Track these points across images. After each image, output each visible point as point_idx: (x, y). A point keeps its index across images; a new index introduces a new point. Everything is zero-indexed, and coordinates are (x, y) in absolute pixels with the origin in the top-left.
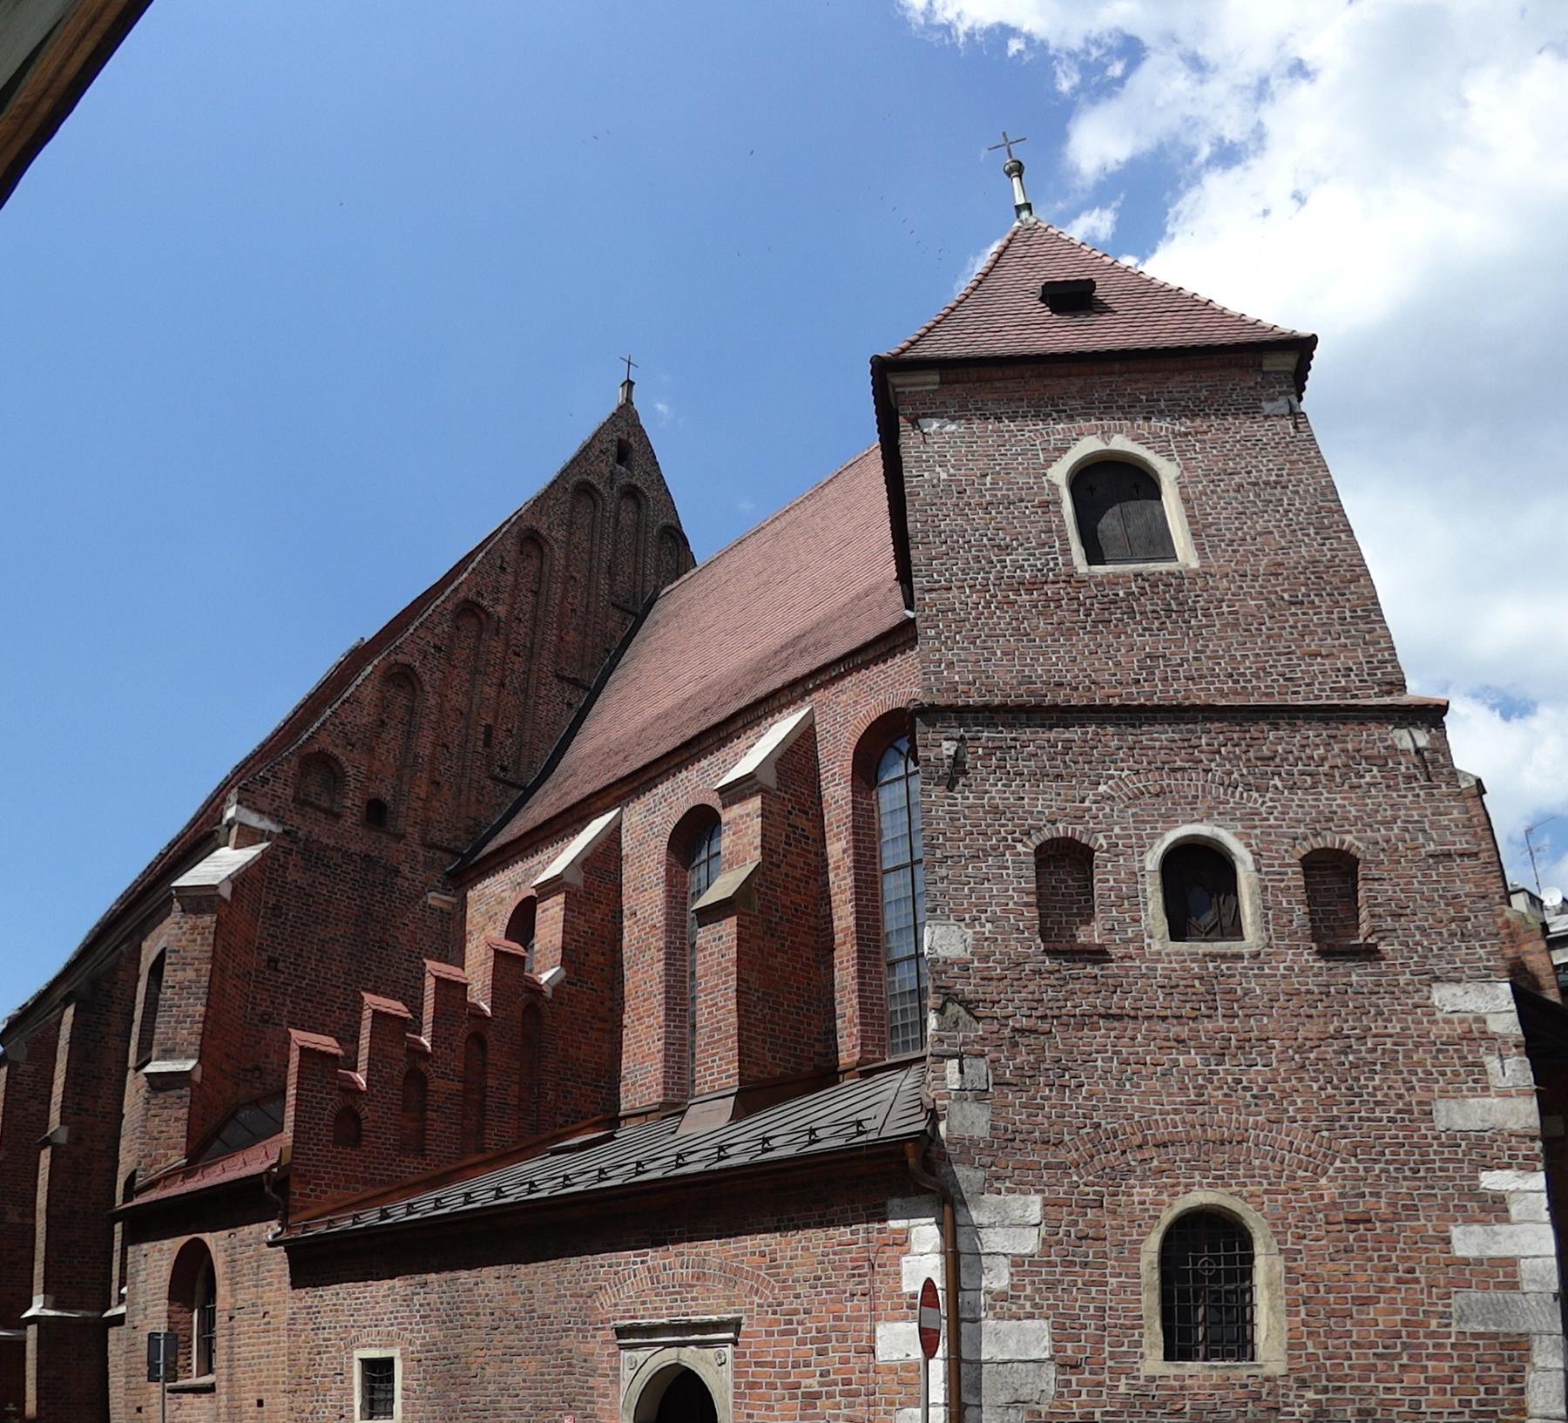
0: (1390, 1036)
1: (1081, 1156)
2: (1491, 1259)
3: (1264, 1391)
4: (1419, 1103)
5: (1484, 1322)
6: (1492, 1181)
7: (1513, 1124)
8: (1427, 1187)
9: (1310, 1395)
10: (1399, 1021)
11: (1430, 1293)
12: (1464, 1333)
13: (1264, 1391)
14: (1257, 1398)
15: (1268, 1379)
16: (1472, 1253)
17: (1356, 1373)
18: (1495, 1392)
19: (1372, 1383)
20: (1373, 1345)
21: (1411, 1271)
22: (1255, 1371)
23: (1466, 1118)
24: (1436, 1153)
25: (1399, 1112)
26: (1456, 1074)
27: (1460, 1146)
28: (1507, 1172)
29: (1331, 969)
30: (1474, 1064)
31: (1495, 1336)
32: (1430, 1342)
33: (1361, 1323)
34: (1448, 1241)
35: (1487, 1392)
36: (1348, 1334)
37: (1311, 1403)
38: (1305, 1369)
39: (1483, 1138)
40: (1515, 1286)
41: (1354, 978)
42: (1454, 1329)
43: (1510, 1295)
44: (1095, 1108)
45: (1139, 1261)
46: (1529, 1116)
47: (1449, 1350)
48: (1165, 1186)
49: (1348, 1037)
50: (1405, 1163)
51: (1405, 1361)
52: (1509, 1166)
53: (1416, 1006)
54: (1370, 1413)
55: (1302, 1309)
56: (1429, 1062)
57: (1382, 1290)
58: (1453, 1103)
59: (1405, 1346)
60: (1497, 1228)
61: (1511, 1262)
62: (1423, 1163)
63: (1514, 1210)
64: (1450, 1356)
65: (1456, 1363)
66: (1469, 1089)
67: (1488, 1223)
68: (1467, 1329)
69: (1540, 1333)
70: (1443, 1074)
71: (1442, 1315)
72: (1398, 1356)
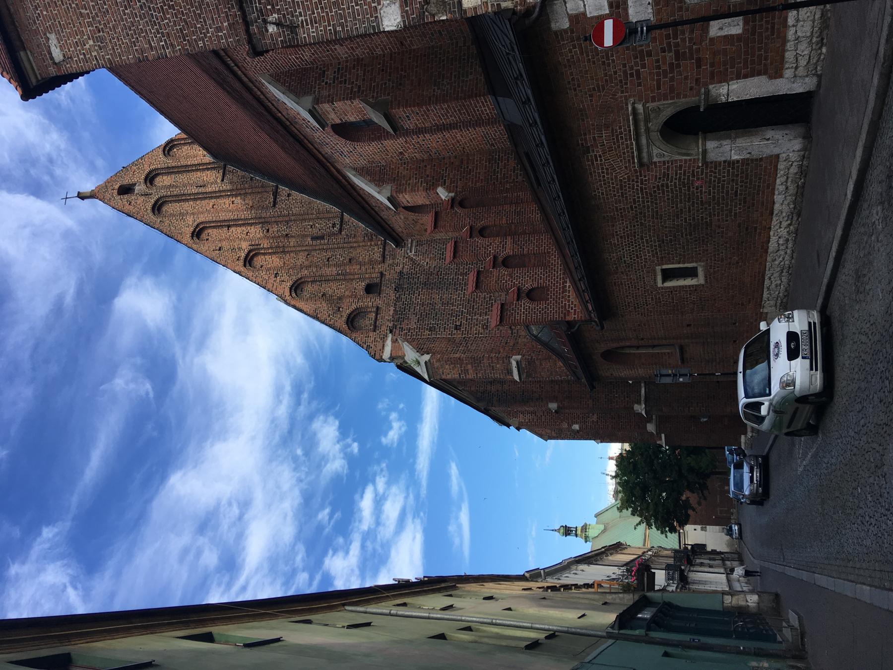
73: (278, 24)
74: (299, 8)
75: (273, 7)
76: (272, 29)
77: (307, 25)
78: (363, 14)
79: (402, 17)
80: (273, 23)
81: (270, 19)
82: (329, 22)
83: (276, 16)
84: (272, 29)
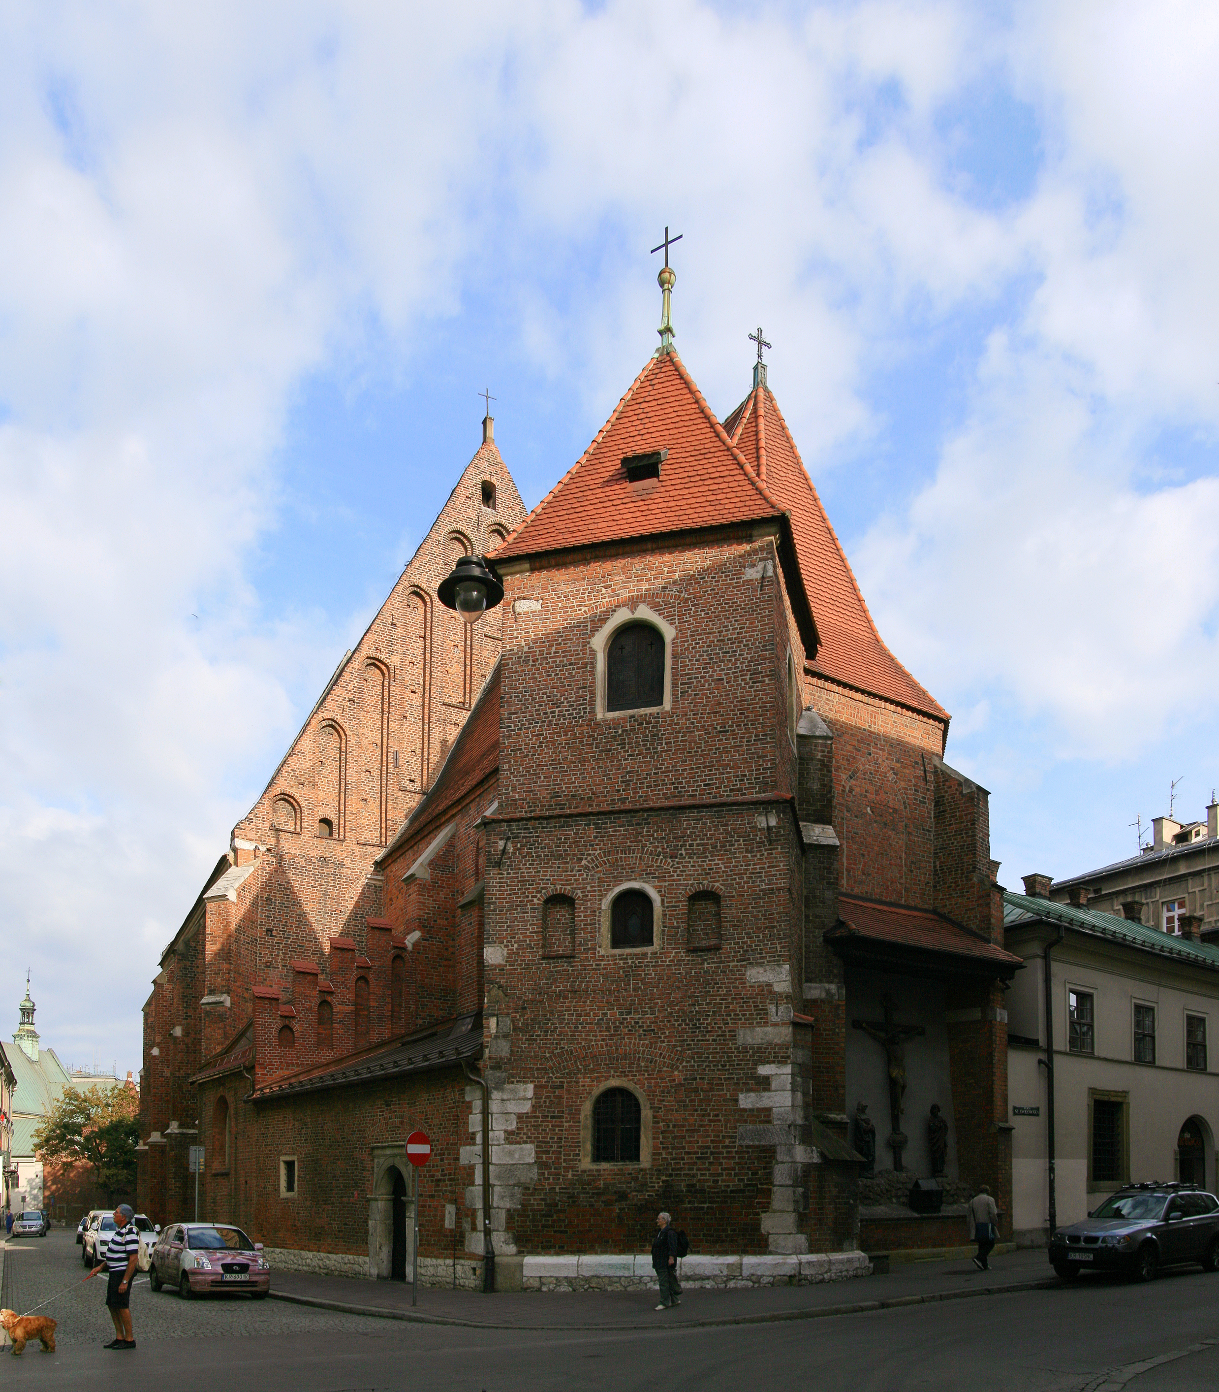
0: (720, 995)
1: (554, 1064)
2: (759, 1110)
3: (640, 1176)
4: (730, 1031)
5: (752, 1140)
6: (764, 1070)
7: (777, 1041)
8: (729, 1074)
9: (664, 1178)
10: (726, 987)
11: (726, 1125)
12: (742, 1146)
13: (640, 1176)
14: (636, 1179)
15: (641, 1170)
16: (749, 1106)
17: (687, 1166)
18: (756, 1174)
19: (695, 1171)
20: (697, 1153)
21: (717, 1115)
22: (637, 1166)
23: (753, 1039)
24: (735, 1056)
25: (718, 1036)
26: (751, 1014)
27: (748, 1052)
28: (772, 1065)
29: (694, 960)
30: (761, 1010)
31: (758, 1146)
32: (725, 1151)
33: (690, 1142)
34: (737, 1101)
35: (752, 1174)
36: (684, 1148)
37: (663, 1181)
38: (661, 1165)
39: (761, 1048)
40: (769, 1122)
41: (706, 965)
42: (737, 1144)
43: (770, 1126)
44: (562, 1039)
45: (579, 1114)
46: (786, 1036)
47: (734, 1155)
48: (596, 1077)
49: (697, 997)
50: (719, 1062)
51: (712, 1160)
52: (773, 1062)
53: (736, 979)
54: (694, 1186)
55: (661, 1136)
56: (738, 1009)
57: (702, 1126)
58: (748, 1031)
59: (712, 1153)
60: (763, 1094)
61: (769, 1110)
62: (729, 1061)
63: (774, 1085)
64: (734, 1157)
65: (737, 1160)
66: (757, 1023)
67: (759, 1091)
68: (744, 1143)
69: (780, 1144)
70: (744, 1015)
71: (731, 1137)
72: (708, 1158)
73: (504, 850)
74: (514, 873)
75: (519, 849)
76: (501, 843)
77: (500, 878)
78: (500, 931)
79: (492, 965)
80: (505, 848)
81: (510, 845)
82: (499, 899)
83: (511, 851)
84: (501, 843)
